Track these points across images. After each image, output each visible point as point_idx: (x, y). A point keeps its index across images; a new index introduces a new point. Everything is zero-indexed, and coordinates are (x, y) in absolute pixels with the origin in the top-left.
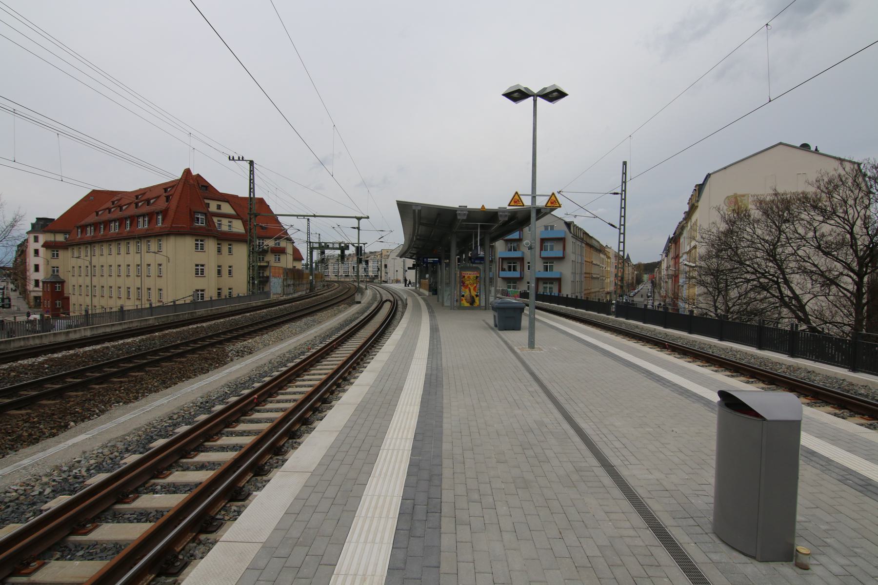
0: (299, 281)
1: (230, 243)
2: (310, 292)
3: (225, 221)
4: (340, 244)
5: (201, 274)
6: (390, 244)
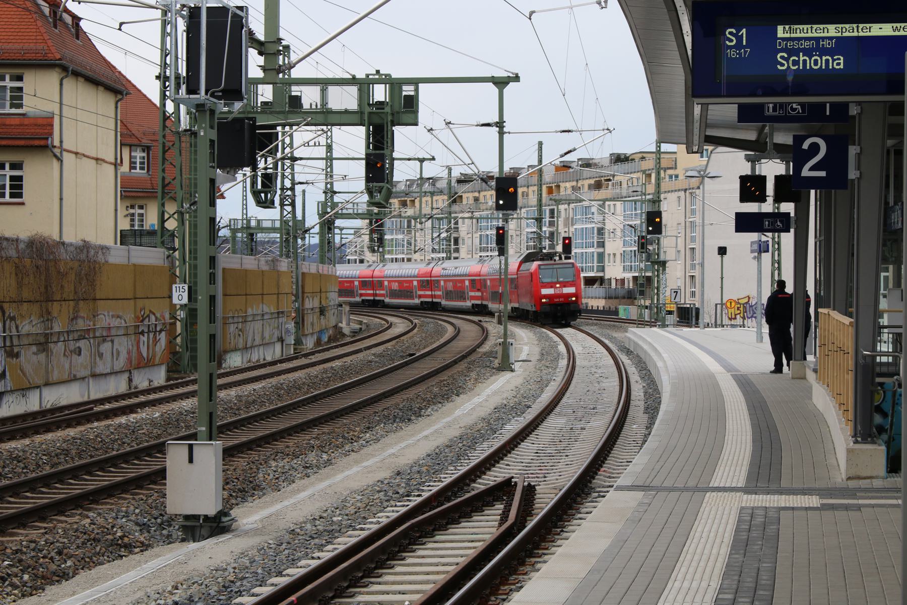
0: (47, 317)
2: (168, 379)
4: (364, 85)
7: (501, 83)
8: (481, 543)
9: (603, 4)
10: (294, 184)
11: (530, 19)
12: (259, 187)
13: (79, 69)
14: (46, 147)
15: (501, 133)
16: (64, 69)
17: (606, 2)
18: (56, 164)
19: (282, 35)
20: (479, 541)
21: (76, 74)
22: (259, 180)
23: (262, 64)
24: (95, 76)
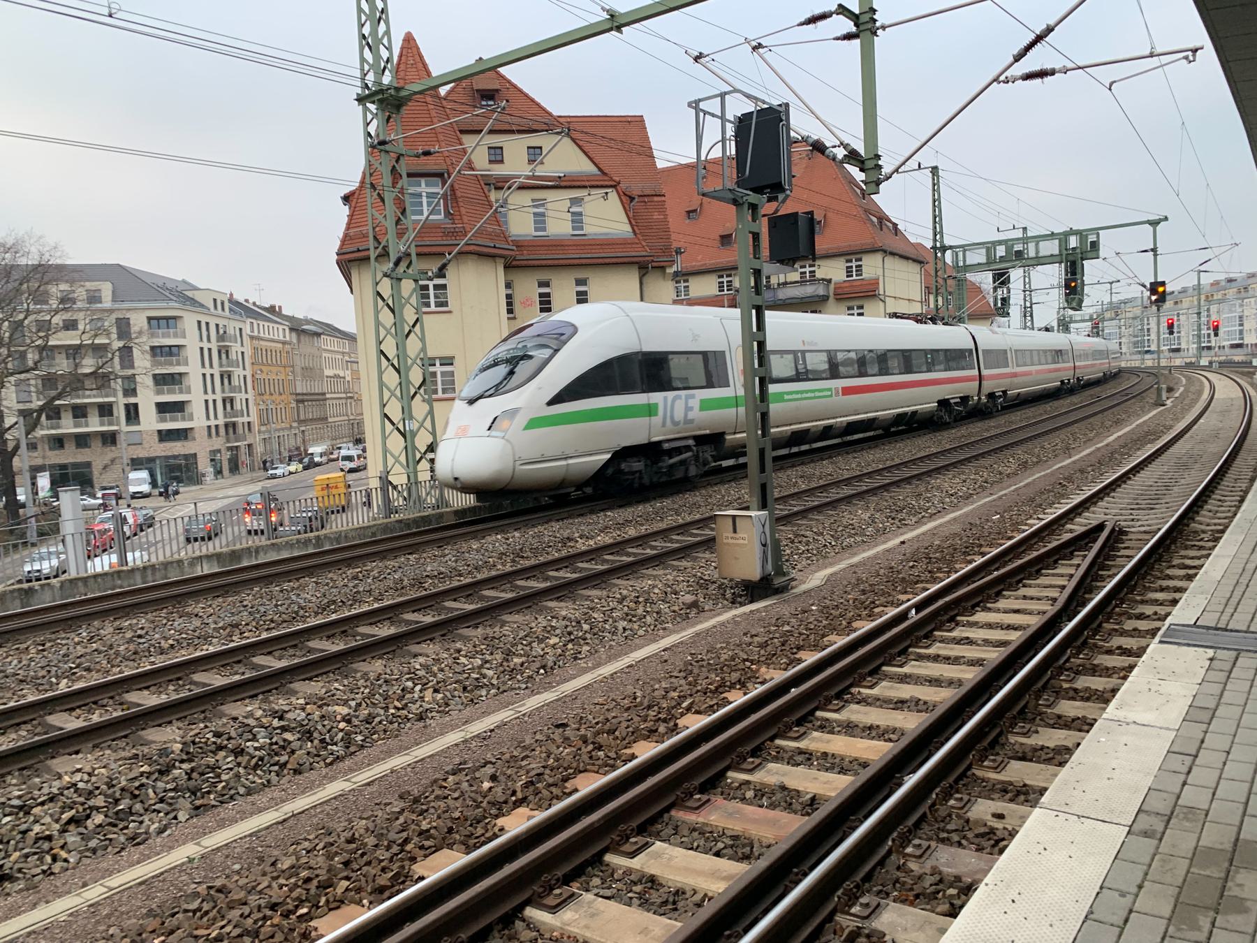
1: (581, 274)
3: (558, 202)
4: (1064, 237)
5: (444, 391)
6: (1105, 74)
7: (1154, 223)
8: (1019, 633)
9: (1191, 58)
10: (1031, 304)
11: (1110, 89)
12: (999, 305)
13: (895, 251)
14: (875, 295)
15: (1155, 255)
16: (885, 251)
17: (1194, 56)
18: (881, 303)
19: (880, 153)
20: (1015, 628)
21: (893, 254)
22: (999, 302)
23: (864, 178)
24: (908, 255)
